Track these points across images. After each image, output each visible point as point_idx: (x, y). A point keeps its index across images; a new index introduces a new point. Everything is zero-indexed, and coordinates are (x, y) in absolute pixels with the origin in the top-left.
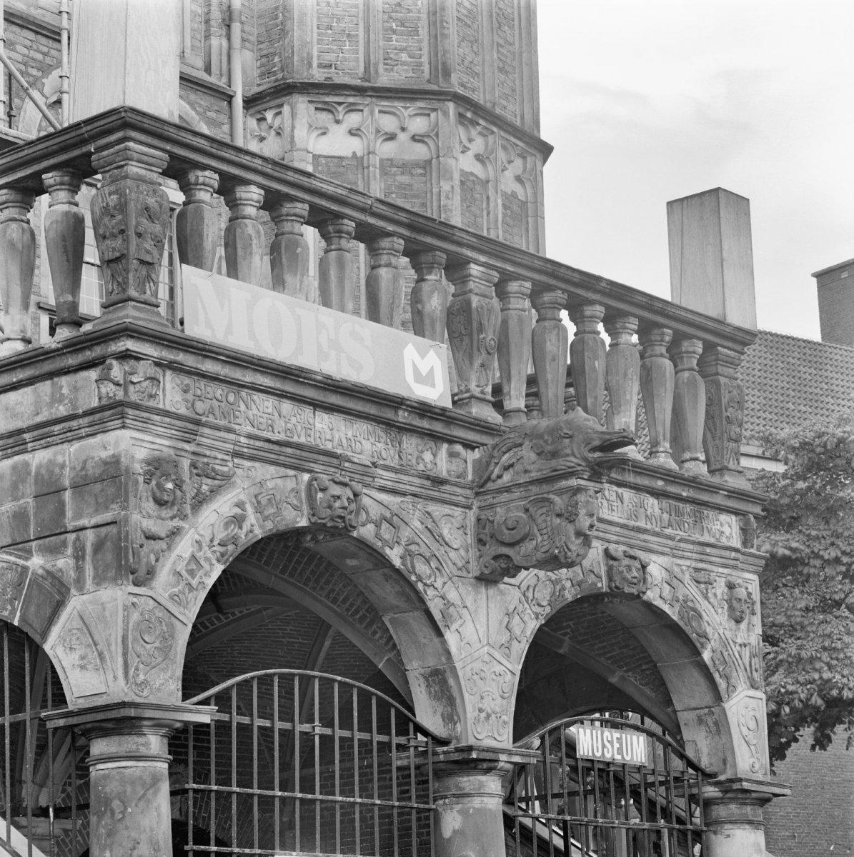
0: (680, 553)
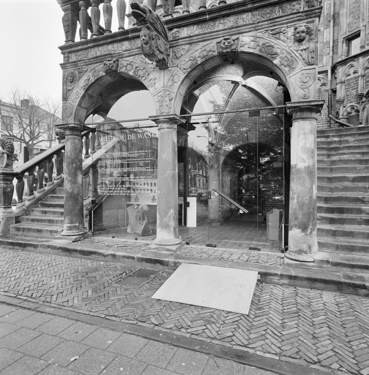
0: (260, 27)
